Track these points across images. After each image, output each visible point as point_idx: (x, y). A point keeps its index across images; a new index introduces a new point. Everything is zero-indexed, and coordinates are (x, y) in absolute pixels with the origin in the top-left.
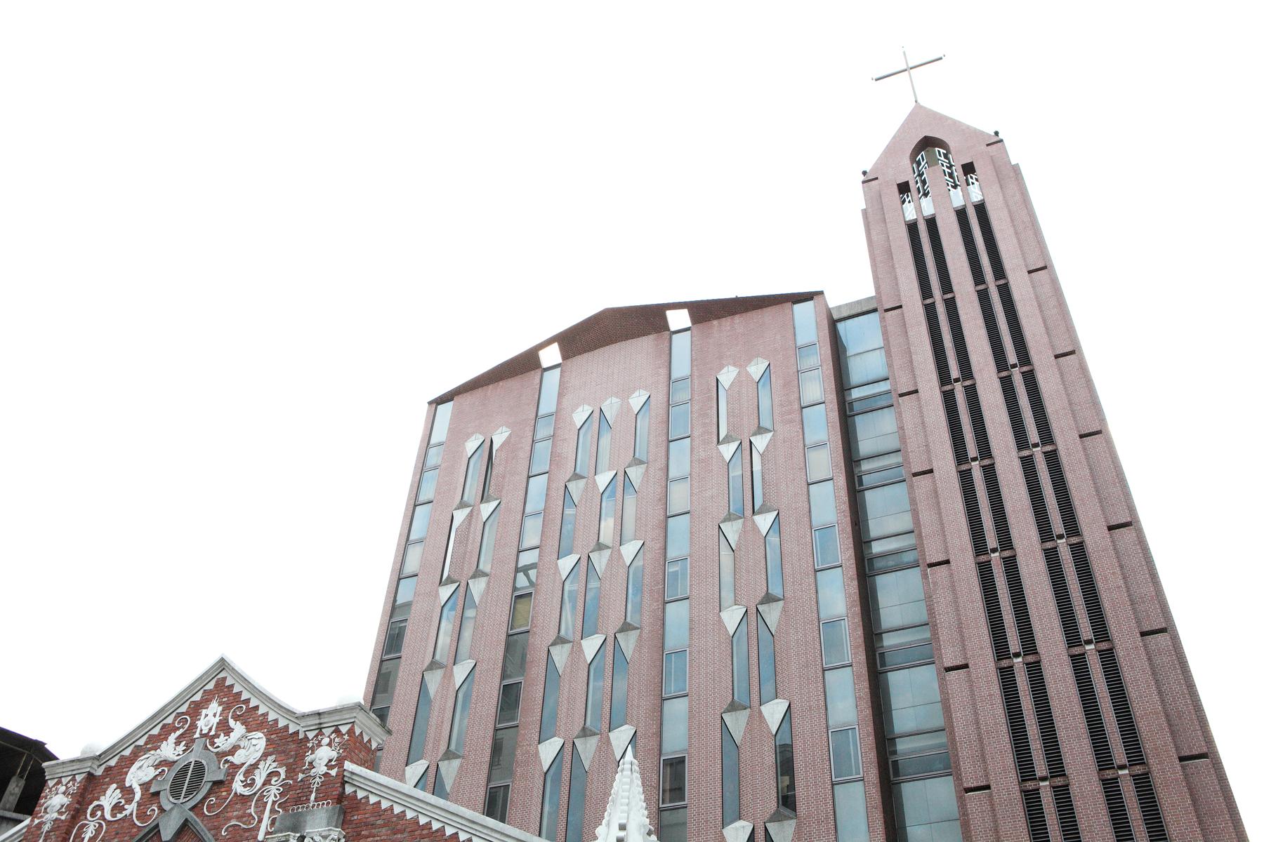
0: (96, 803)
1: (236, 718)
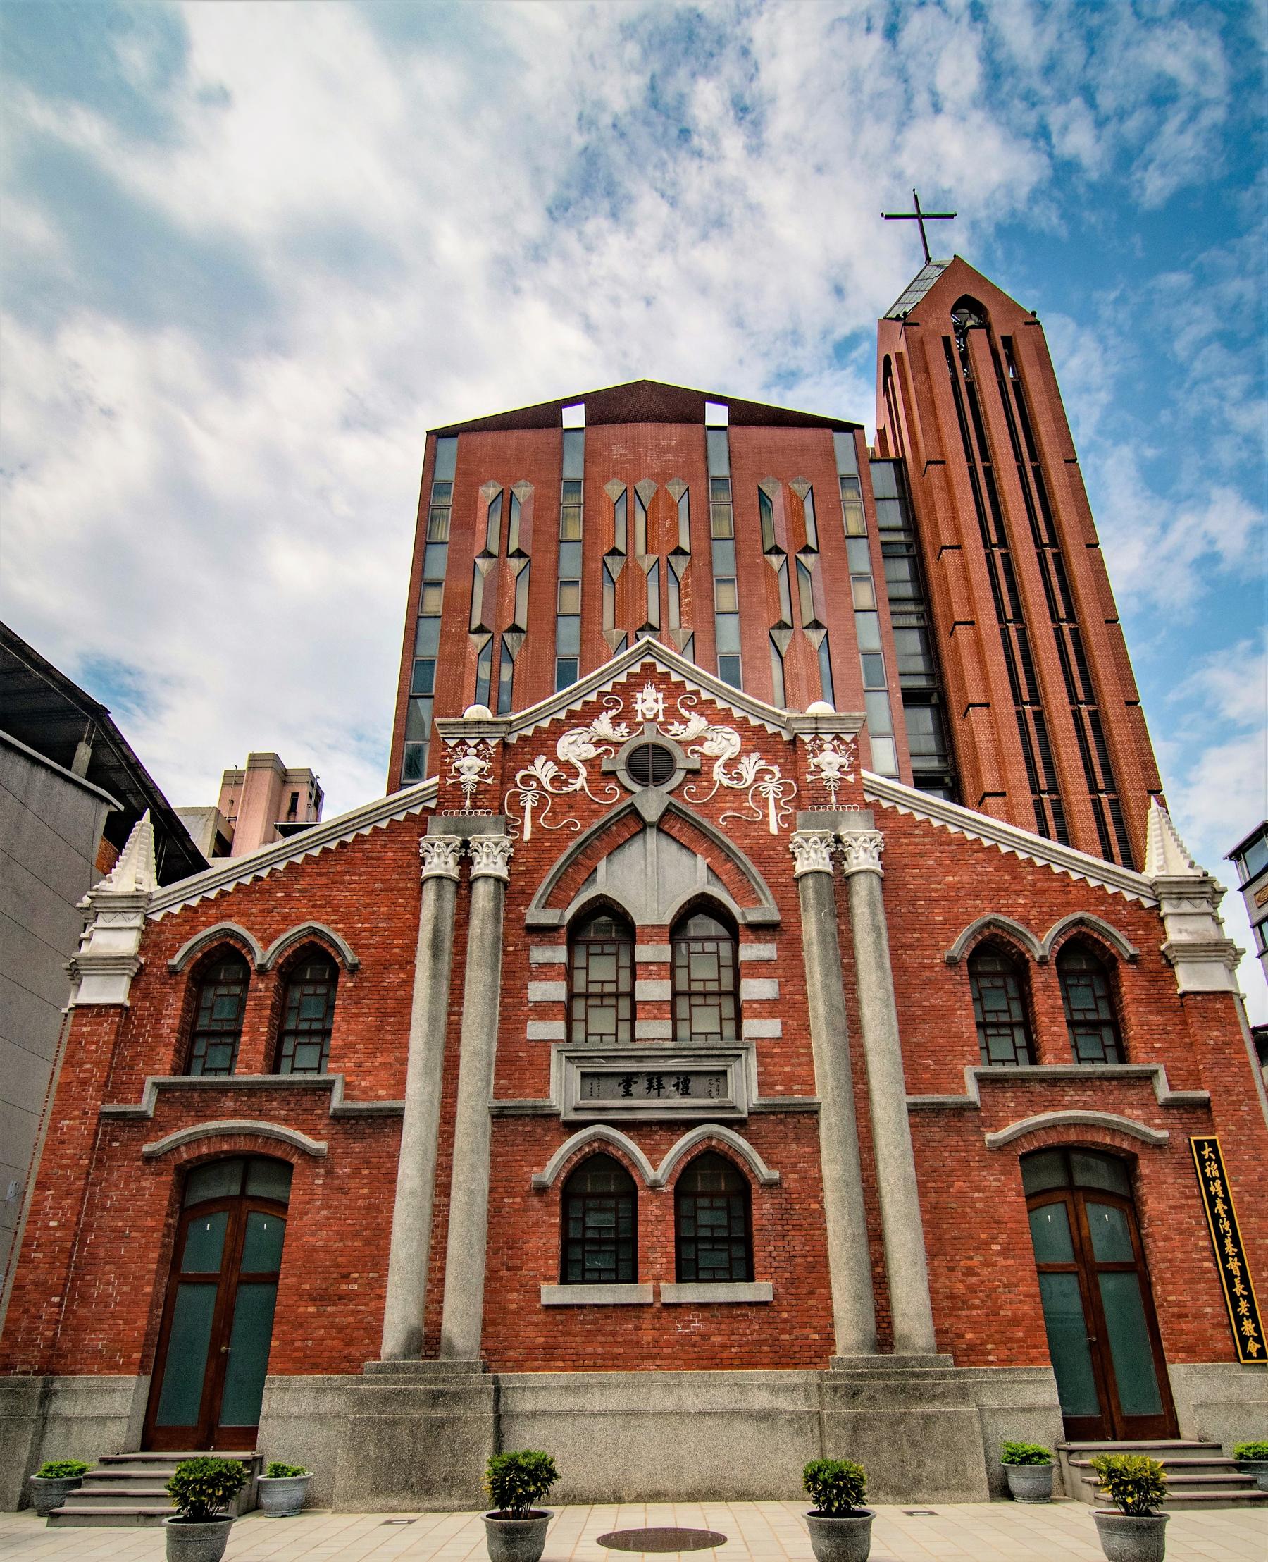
0: (523, 772)
1: (689, 708)
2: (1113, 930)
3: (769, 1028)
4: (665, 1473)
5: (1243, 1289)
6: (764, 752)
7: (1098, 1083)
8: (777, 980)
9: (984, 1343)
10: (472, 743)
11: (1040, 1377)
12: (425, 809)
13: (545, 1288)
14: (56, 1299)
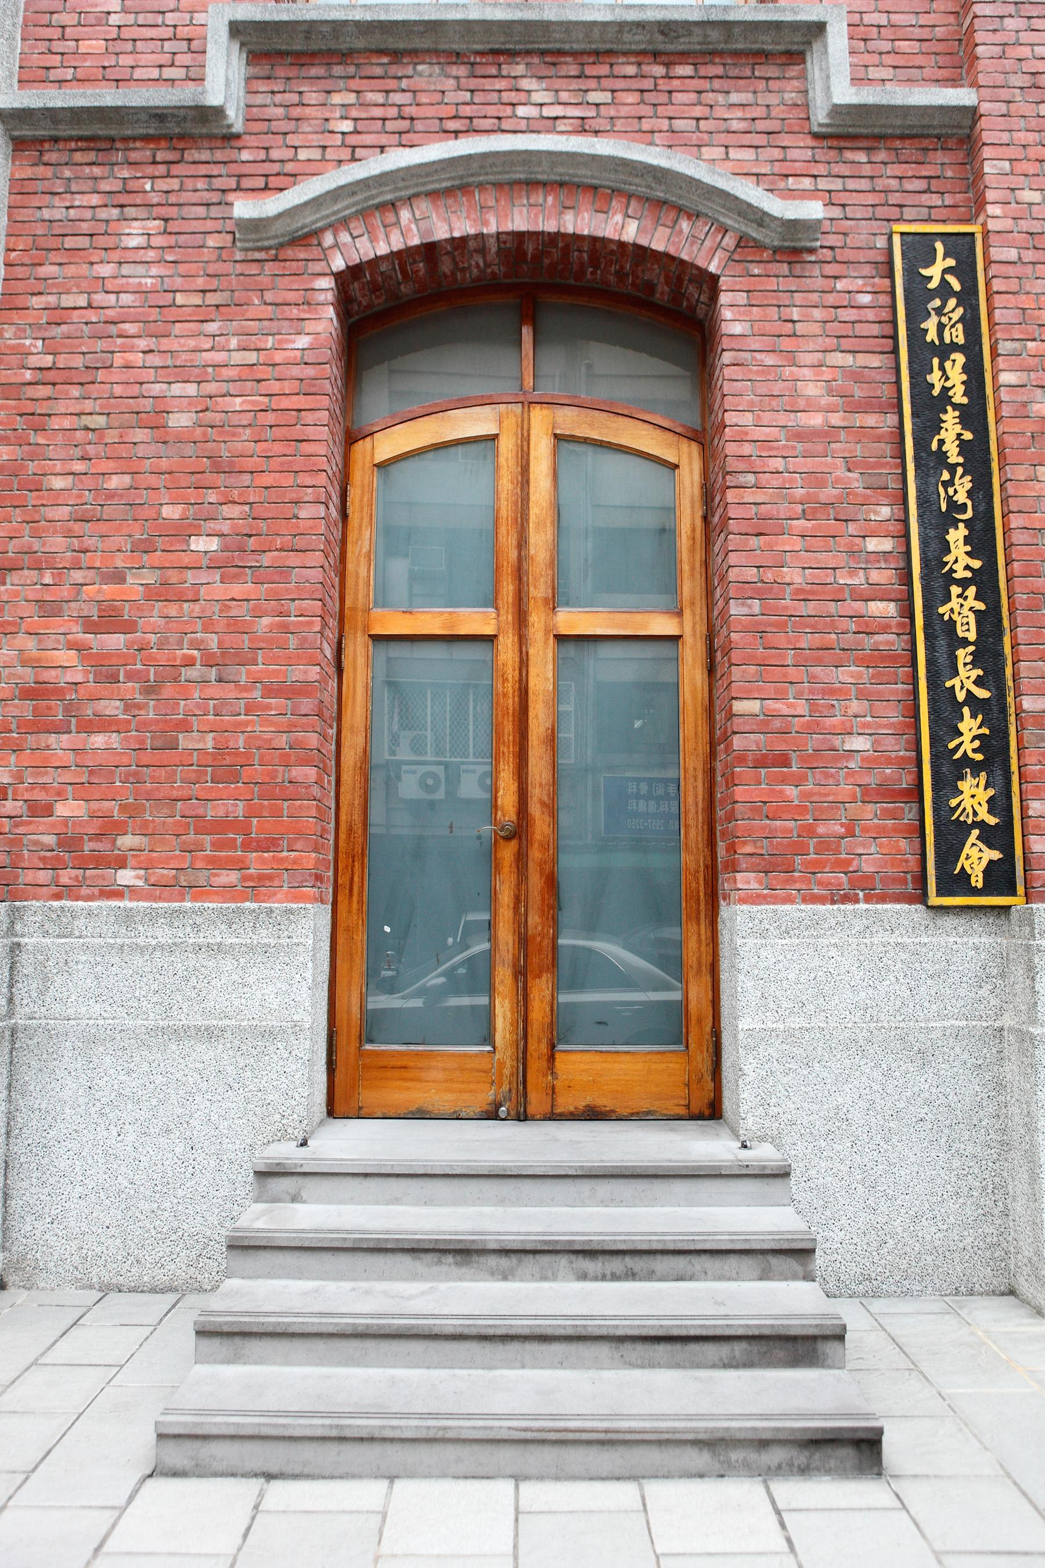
5: (979, 682)
7: (631, 70)
9: (111, 829)
11: (264, 936)
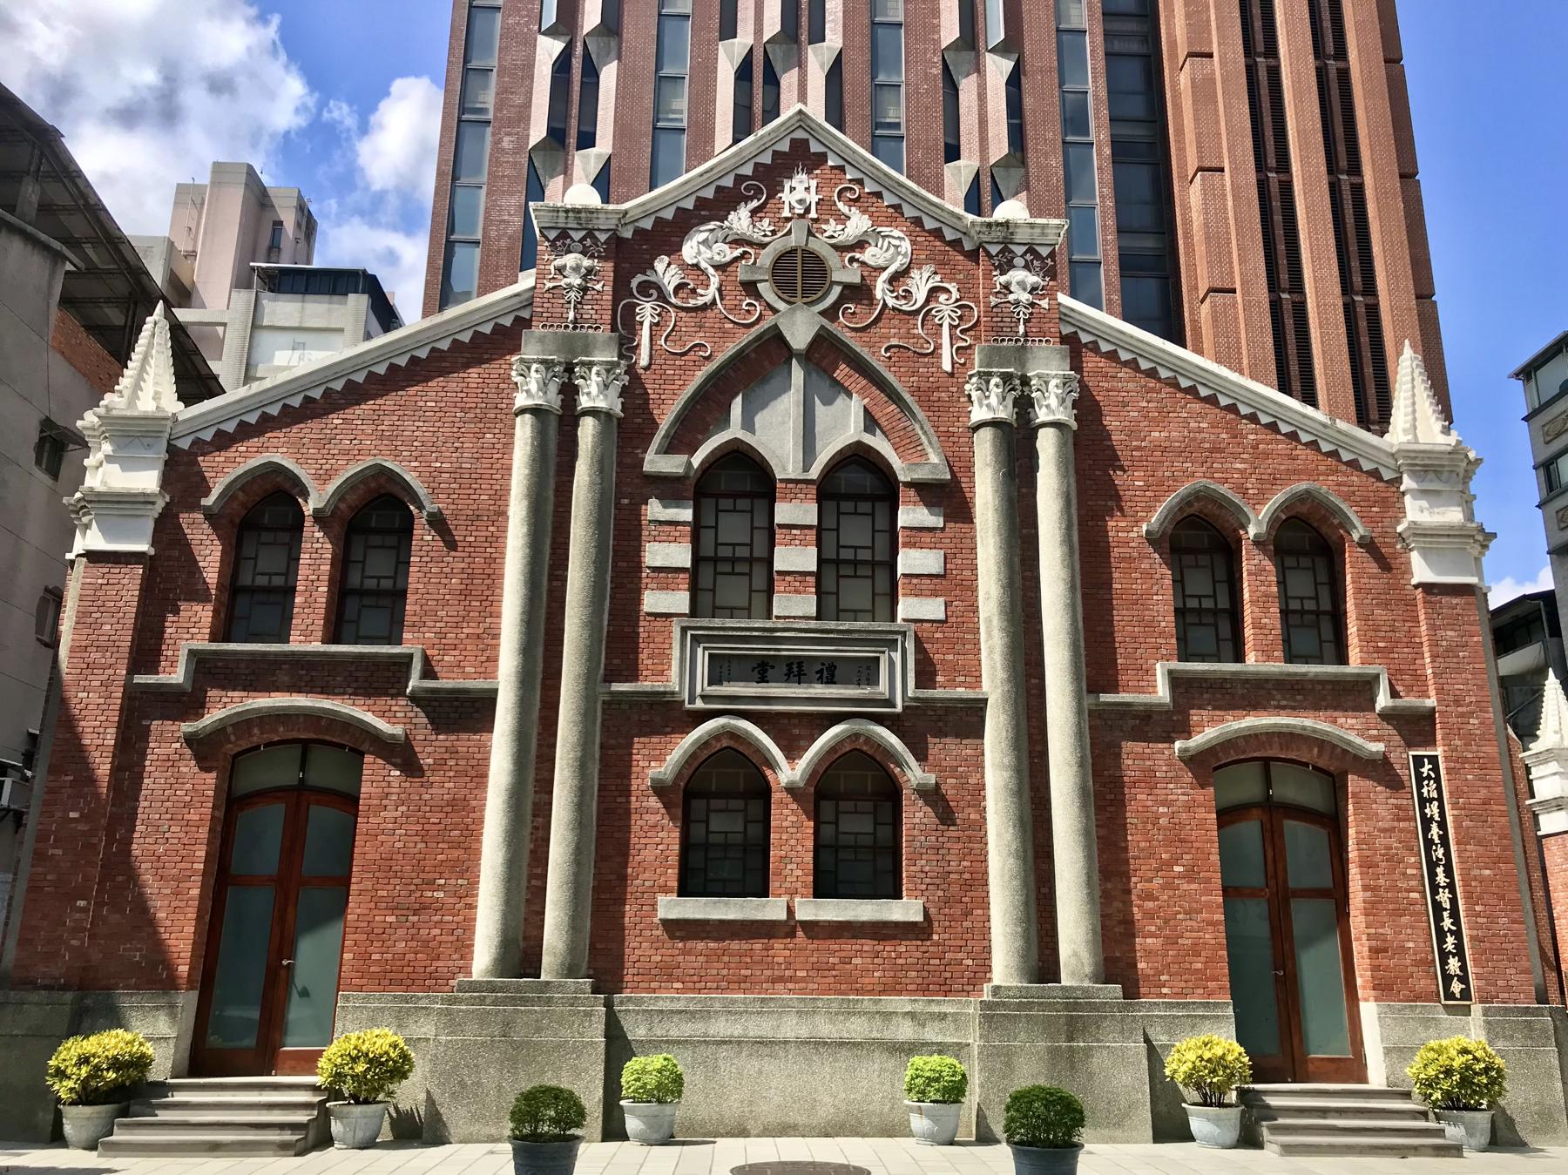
0: (640, 278)
2: (1344, 506)
3: (933, 609)
4: (796, 1106)
6: (941, 265)
8: (942, 552)
10: (577, 236)
12: (517, 319)
13: (662, 899)
14: (81, 903)
